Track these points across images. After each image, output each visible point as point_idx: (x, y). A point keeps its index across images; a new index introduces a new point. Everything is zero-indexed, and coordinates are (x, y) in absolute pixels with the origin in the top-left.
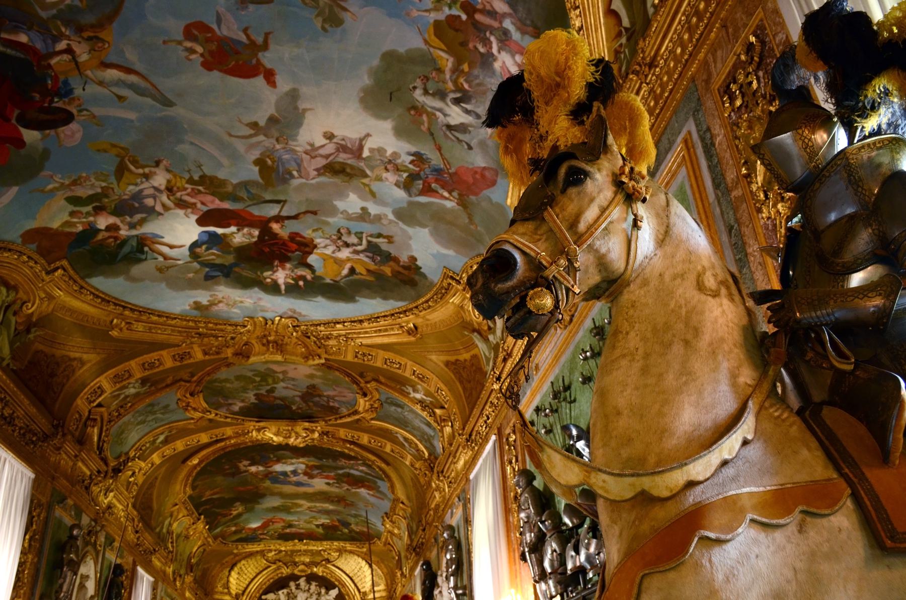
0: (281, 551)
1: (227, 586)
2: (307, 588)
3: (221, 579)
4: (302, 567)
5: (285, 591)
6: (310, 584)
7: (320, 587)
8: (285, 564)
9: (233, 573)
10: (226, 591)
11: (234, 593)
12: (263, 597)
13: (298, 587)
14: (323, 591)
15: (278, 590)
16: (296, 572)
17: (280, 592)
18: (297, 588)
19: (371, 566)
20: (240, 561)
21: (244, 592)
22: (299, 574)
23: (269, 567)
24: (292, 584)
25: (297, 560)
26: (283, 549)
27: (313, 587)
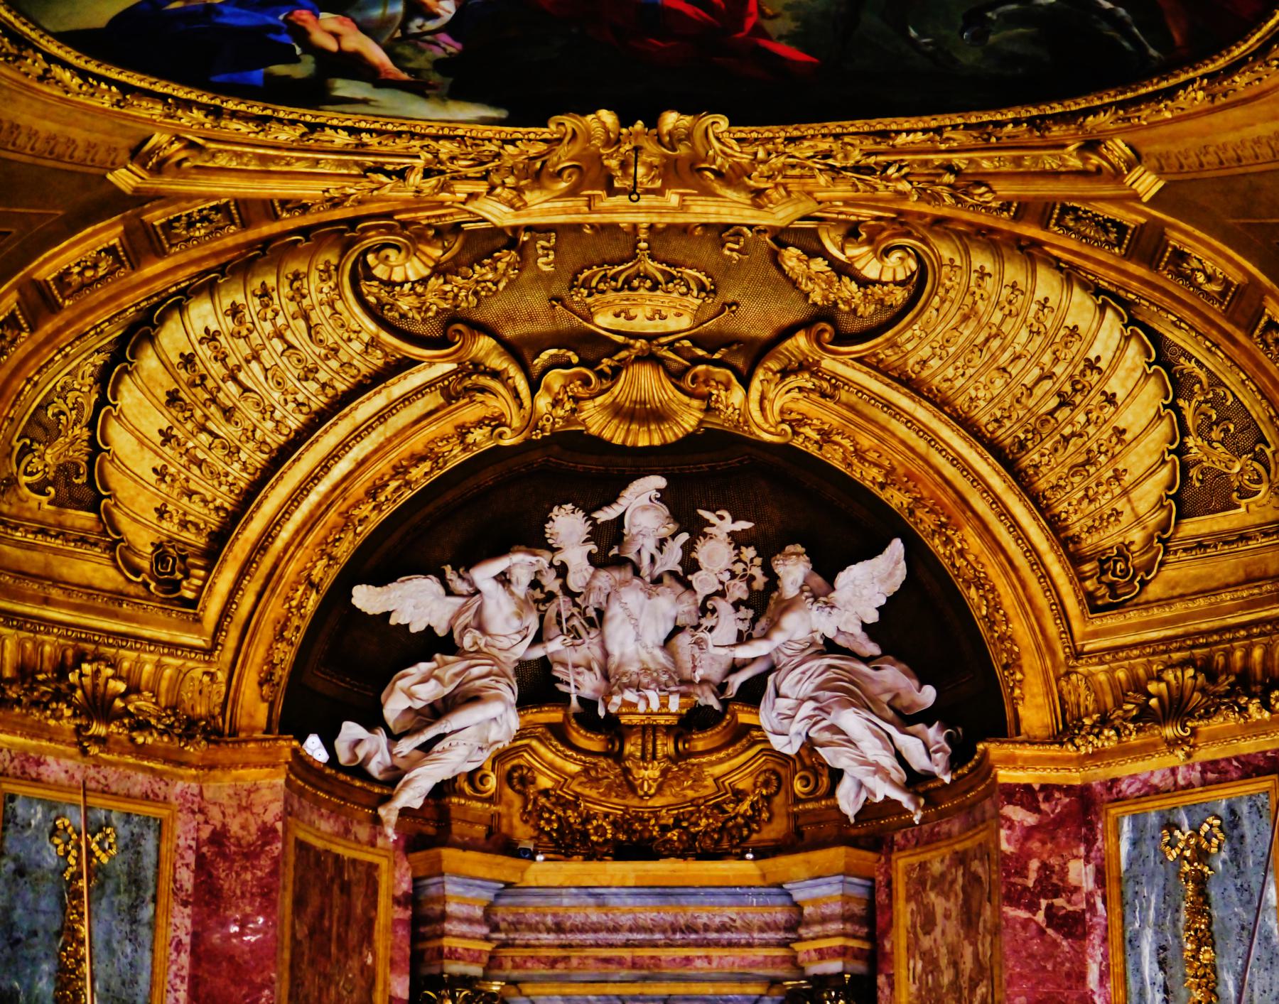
0: (486, 243)
1: (86, 486)
2: (672, 558)
3: (42, 428)
4: (647, 383)
5: (521, 564)
6: (697, 529)
7: (769, 547)
8: (516, 350)
9: (129, 396)
10: (82, 519)
11: (142, 539)
12: (366, 598)
13: (609, 546)
14: (794, 571)
15: (467, 560)
16: (594, 418)
17: (484, 574)
18: (597, 562)
19: (1163, 357)
20: (178, 302)
21: (219, 539)
22: (616, 433)
23: (406, 364)
24: (567, 526)
25: (604, 320)
26: (497, 213)
27: (716, 554)
